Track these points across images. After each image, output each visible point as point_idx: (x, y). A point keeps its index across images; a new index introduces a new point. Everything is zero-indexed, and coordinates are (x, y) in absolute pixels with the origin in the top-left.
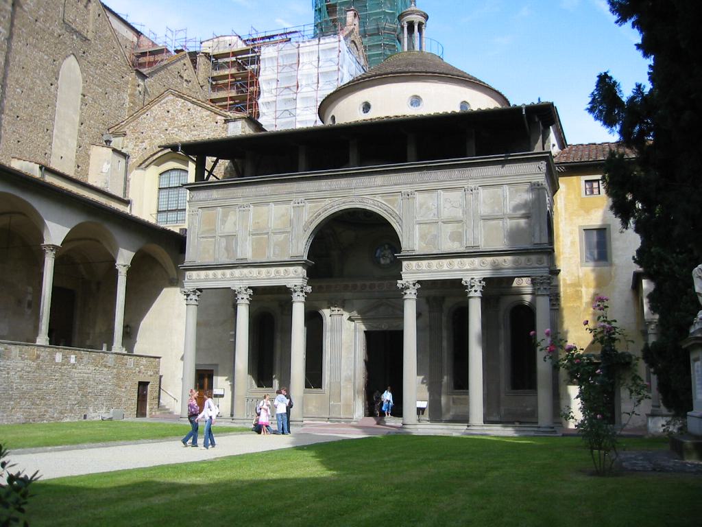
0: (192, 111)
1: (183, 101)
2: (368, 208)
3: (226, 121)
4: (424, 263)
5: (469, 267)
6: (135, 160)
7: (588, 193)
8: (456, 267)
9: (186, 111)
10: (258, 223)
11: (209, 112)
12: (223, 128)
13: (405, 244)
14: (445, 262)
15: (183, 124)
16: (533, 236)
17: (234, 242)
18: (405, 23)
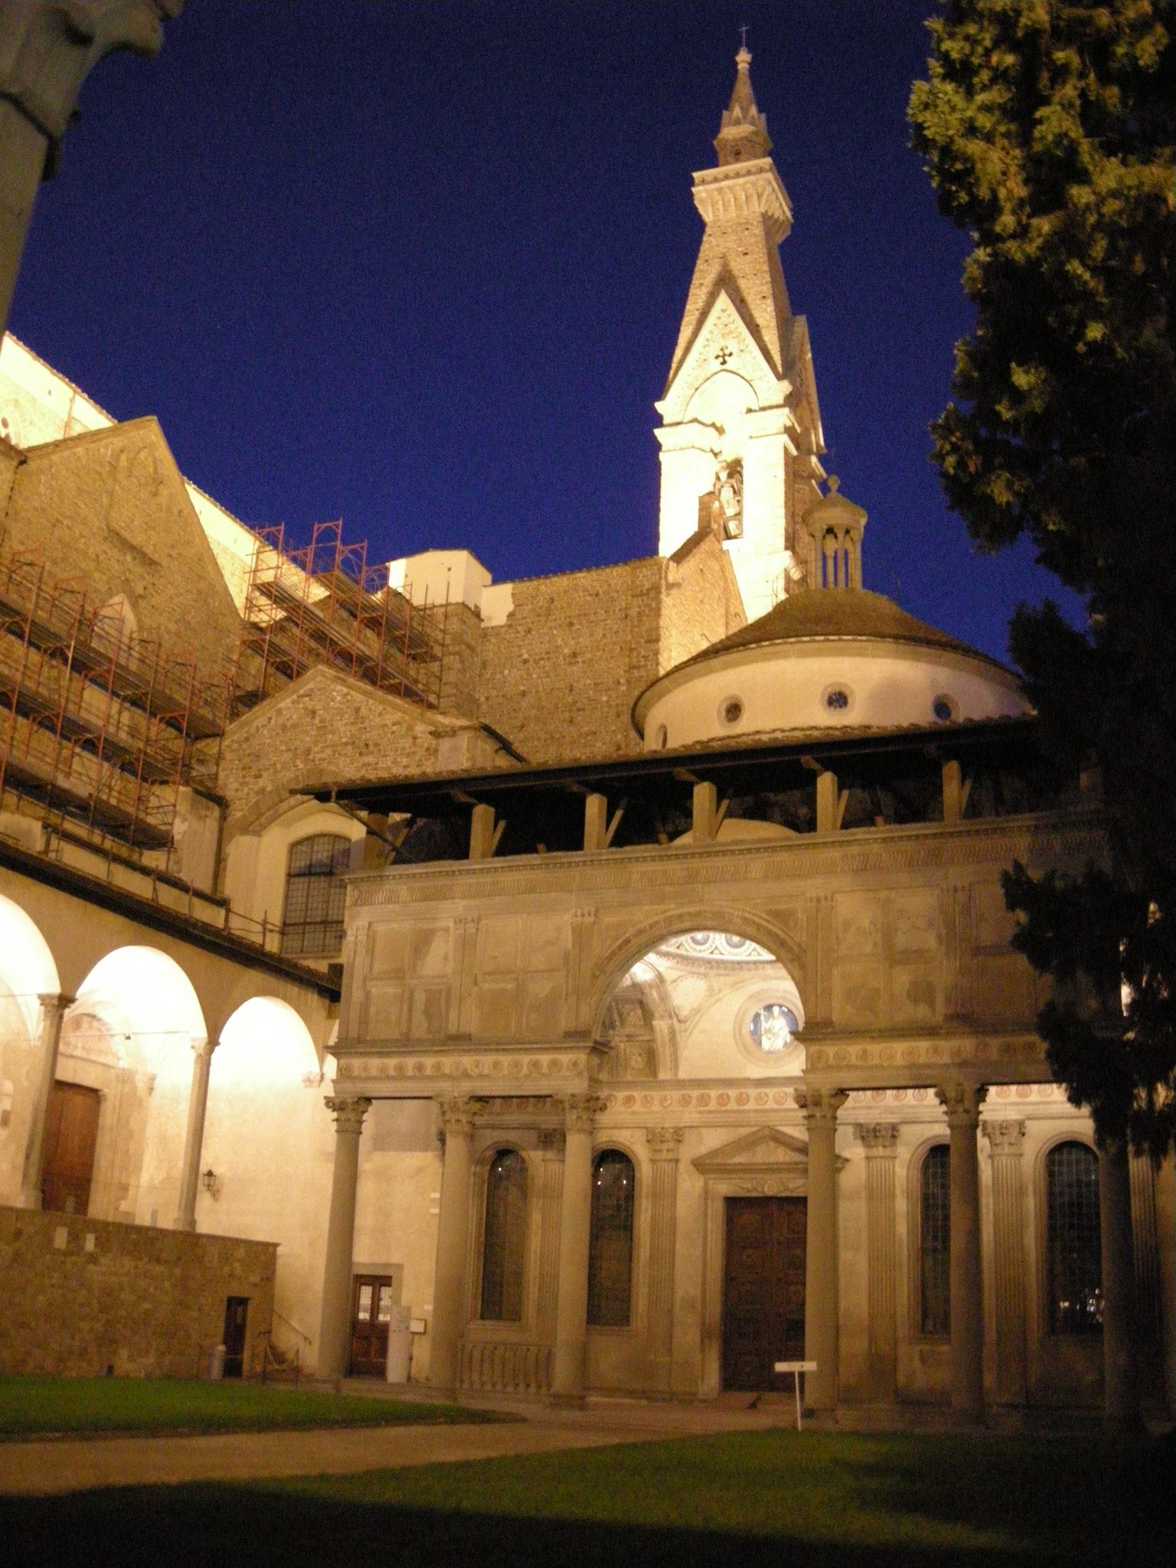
0: (364, 711)
1: (345, 690)
6: (239, 814)
12: (428, 749)
15: (344, 740)
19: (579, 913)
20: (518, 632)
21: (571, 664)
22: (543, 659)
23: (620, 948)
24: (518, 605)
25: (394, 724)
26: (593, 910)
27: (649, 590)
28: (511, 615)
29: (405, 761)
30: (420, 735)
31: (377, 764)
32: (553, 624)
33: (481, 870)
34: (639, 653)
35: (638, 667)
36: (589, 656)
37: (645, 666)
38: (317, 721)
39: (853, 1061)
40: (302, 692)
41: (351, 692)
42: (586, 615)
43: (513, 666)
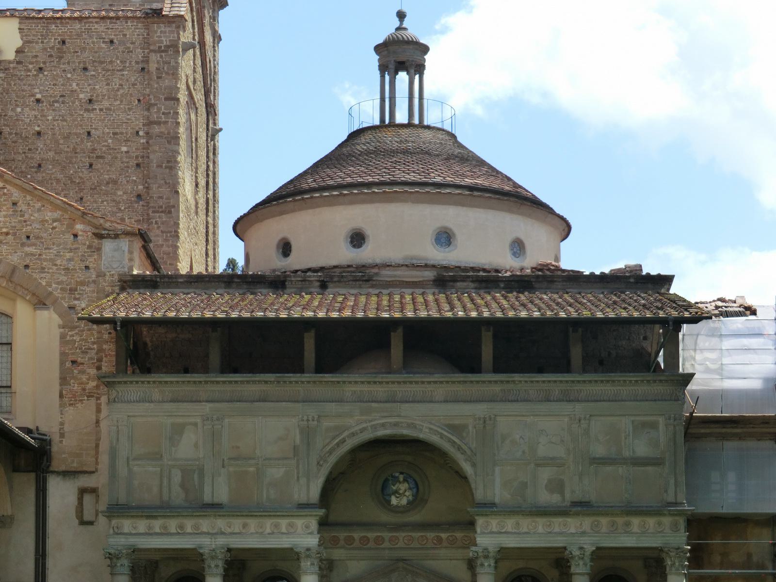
0: (22, 206)
2: (421, 436)
3: (100, 236)
4: (510, 523)
5: (573, 530)
8: (557, 530)
9: (10, 205)
10: (238, 447)
11: (57, 214)
12: (90, 247)
13: (479, 495)
14: (541, 524)
16: (666, 491)
17: (196, 476)
18: (392, 62)
19: (305, 418)
20: (30, 71)
21: (87, 110)
22: (57, 102)
23: (338, 445)
24: (26, 42)
26: (316, 417)
27: (167, 47)
28: (19, 51)
29: (68, 255)
30: (80, 233)
31: (40, 255)
33: (224, 382)
34: (159, 109)
35: (158, 123)
36: (106, 104)
37: (166, 123)
39: (510, 530)
42: (101, 63)
43: (24, 105)
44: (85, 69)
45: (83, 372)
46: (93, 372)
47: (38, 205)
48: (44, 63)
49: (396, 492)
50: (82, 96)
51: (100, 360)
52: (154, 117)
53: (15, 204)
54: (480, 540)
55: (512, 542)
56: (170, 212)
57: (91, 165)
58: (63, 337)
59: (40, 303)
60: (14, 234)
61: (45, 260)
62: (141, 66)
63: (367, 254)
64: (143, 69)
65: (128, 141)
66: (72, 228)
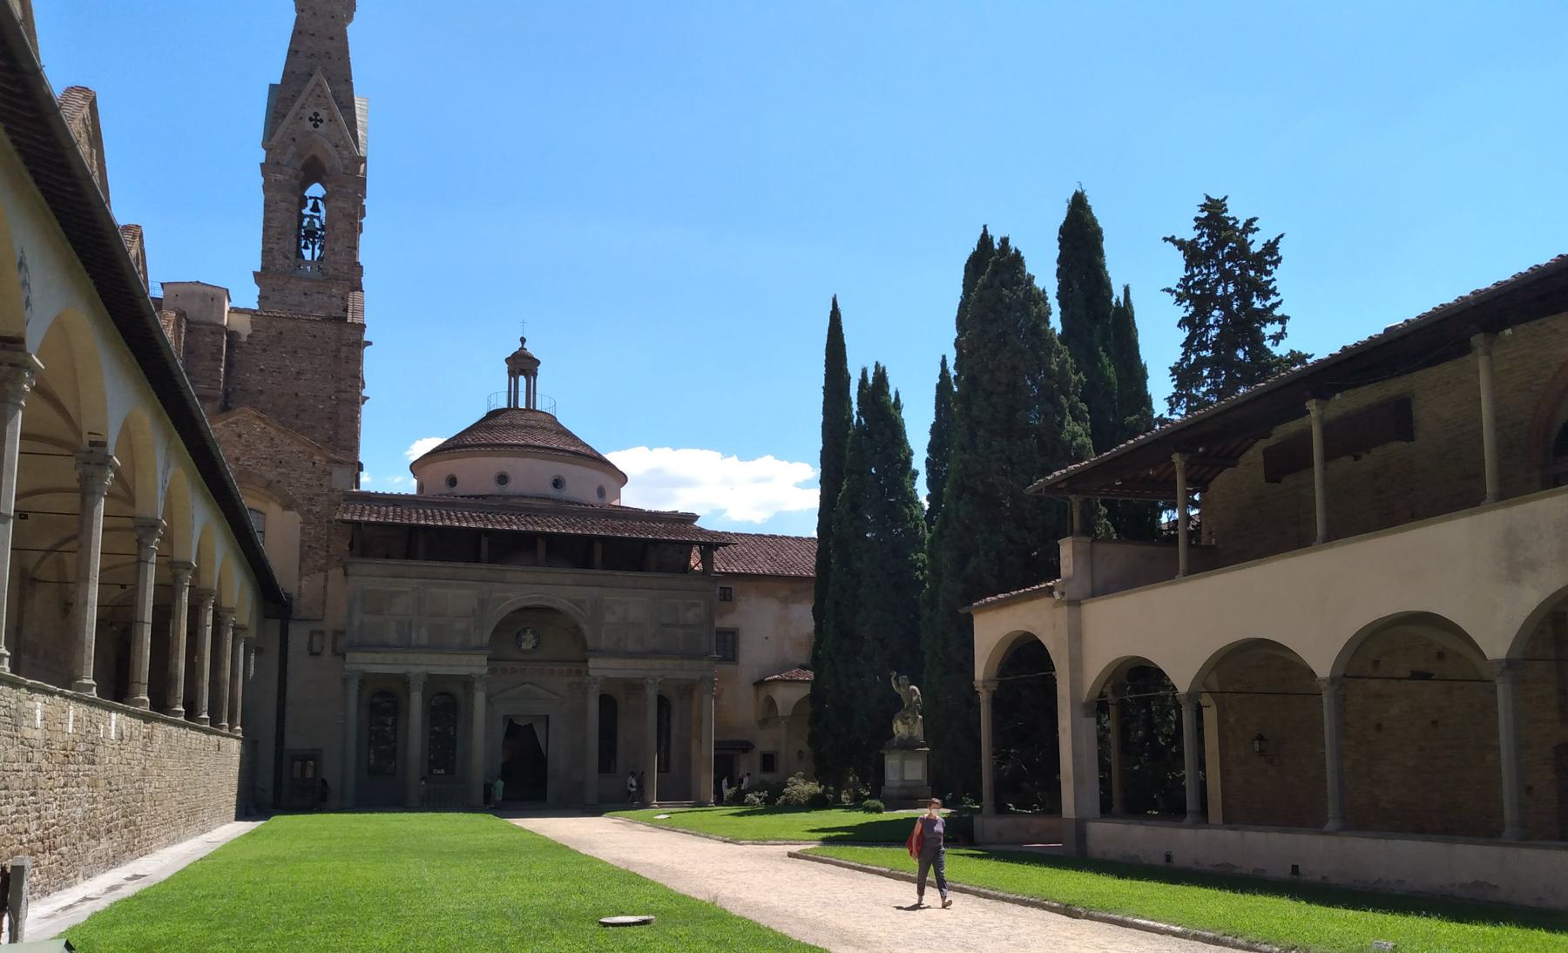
0: (277, 441)
1: (263, 426)
2: (555, 606)
7: (722, 597)
13: (591, 644)
14: (630, 663)
21: (296, 379)
22: (275, 371)
25: (300, 452)
29: (309, 476)
32: (283, 350)
33: (428, 566)
35: (346, 392)
36: (309, 376)
38: (243, 441)
40: (229, 420)
41: (268, 427)
42: (308, 349)
44: (296, 352)
45: (316, 553)
46: (323, 553)
47: (289, 441)
48: (267, 346)
49: (524, 640)
50: (292, 369)
51: (328, 546)
52: (343, 387)
53: (272, 439)
54: (591, 672)
55: (611, 674)
56: (352, 451)
57: (297, 416)
58: (302, 529)
59: (288, 505)
60: (271, 460)
61: (292, 478)
62: (334, 354)
63: (511, 488)
64: (336, 356)
65: (323, 401)
66: (312, 457)
